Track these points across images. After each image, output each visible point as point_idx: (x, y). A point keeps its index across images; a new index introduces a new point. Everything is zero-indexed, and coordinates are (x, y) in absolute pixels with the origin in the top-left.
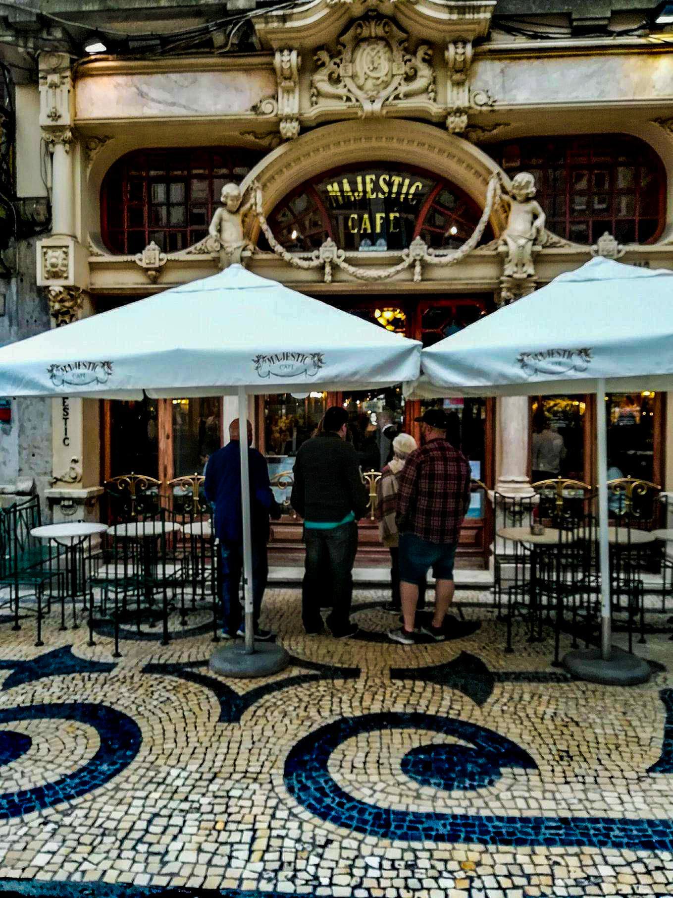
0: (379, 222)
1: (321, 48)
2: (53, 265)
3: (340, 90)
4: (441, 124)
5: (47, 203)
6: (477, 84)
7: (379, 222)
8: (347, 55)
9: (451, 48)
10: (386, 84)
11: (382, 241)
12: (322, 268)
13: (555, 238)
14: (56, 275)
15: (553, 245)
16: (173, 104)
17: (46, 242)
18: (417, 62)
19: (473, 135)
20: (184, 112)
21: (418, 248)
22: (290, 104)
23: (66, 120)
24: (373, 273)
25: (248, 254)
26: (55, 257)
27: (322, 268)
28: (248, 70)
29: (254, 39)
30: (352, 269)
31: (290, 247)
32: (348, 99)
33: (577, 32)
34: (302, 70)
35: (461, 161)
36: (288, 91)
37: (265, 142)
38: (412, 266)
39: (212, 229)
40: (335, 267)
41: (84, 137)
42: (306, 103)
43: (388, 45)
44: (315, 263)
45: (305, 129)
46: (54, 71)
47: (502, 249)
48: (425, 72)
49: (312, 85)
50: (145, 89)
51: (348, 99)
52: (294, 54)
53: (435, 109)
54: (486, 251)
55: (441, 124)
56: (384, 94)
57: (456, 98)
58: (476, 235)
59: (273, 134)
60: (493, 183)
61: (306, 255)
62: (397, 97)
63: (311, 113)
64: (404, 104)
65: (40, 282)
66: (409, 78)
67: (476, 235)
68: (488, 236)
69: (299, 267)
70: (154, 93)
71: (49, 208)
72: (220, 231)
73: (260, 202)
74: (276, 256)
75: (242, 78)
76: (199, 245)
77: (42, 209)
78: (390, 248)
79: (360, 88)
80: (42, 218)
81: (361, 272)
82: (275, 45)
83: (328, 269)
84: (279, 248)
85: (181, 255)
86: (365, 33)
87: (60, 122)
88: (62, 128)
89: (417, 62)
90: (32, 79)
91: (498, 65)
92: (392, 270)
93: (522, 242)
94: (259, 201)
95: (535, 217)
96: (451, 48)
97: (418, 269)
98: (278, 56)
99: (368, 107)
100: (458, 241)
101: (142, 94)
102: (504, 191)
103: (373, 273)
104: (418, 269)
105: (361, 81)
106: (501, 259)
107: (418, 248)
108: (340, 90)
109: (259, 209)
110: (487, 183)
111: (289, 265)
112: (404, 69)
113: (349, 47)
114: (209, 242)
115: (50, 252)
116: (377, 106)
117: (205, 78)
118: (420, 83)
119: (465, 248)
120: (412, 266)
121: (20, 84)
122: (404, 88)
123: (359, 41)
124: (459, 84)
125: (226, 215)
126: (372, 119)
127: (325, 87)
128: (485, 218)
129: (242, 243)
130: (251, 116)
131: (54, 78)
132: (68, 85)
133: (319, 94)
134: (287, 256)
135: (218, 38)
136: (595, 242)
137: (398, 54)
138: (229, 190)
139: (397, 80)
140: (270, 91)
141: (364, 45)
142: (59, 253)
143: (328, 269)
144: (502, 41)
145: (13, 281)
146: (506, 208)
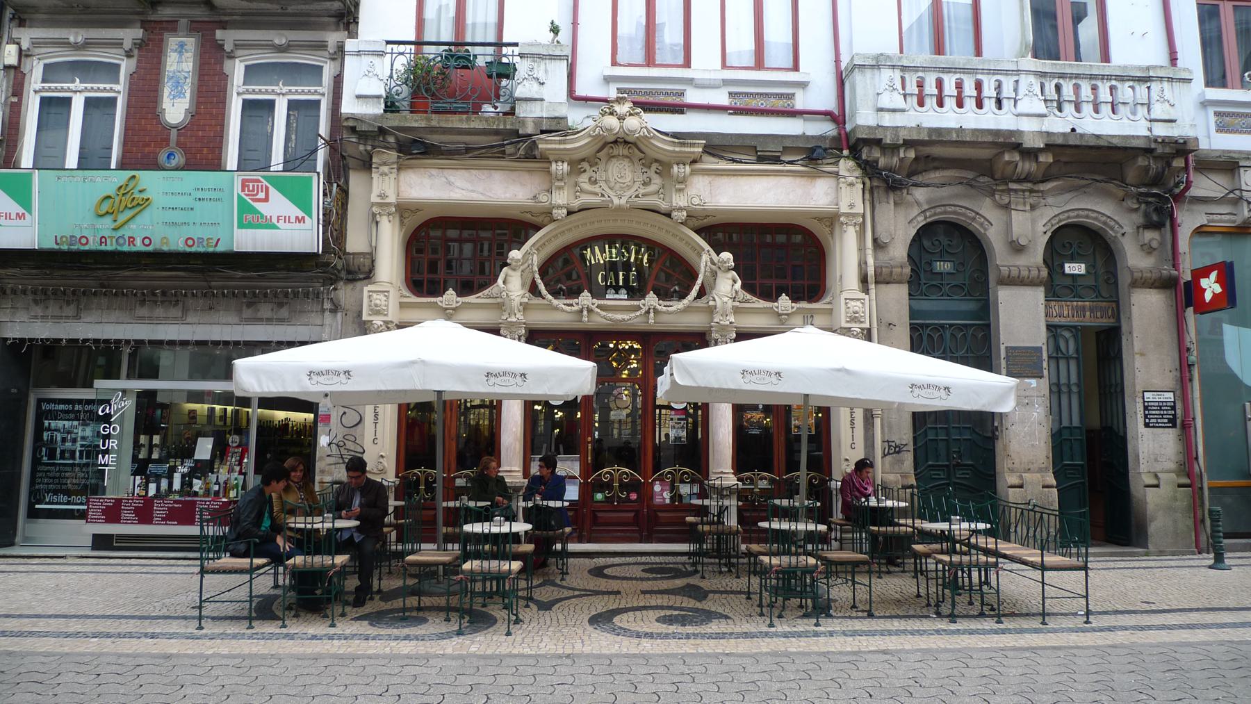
0: (621, 277)
1: (583, 160)
2: (376, 305)
3: (596, 189)
4: (668, 215)
5: (371, 257)
6: (692, 191)
7: (621, 277)
8: (602, 166)
9: (675, 167)
10: (629, 187)
11: (624, 291)
12: (581, 311)
13: (749, 296)
14: (378, 313)
15: (748, 301)
16: (473, 191)
17: (370, 287)
18: (651, 173)
19: (690, 223)
20: (482, 198)
21: (651, 299)
22: (562, 198)
23: (392, 199)
24: (619, 316)
25: (526, 300)
26: (379, 299)
27: (581, 311)
28: (530, 171)
29: (536, 153)
30: (603, 313)
31: (556, 294)
32: (603, 195)
33: (761, 160)
34: (570, 174)
35: (682, 239)
36: (560, 188)
37: (538, 220)
38: (648, 312)
39: (500, 281)
40: (590, 311)
41: (403, 210)
42: (572, 197)
43: (631, 161)
44: (576, 308)
45: (570, 213)
46: (385, 164)
47: (711, 303)
48: (657, 181)
49: (576, 184)
50: (452, 179)
51: (603, 195)
52: (566, 165)
53: (664, 206)
54: (701, 303)
55: (668, 215)
56: (628, 194)
57: (680, 201)
58: (694, 293)
59: (548, 214)
60: (705, 257)
61: (568, 301)
62: (637, 196)
63: (576, 204)
64: (643, 201)
65: (365, 318)
66: (645, 184)
67: (694, 293)
68: (702, 293)
69: (563, 311)
70: (458, 183)
71: (373, 261)
72: (504, 282)
73: (536, 261)
74: (545, 302)
75: (526, 177)
76: (486, 292)
77: (368, 262)
78: (631, 297)
79: (611, 189)
80: (367, 269)
81: (609, 315)
82: (551, 158)
83: (585, 313)
84: (550, 297)
85: (471, 299)
86: (615, 152)
87: (387, 201)
88: (388, 205)
89: (651, 173)
90: (366, 165)
91: (707, 179)
92: (633, 315)
93: (726, 299)
94: (535, 263)
95: (735, 282)
96: (675, 167)
97: (652, 315)
98: (554, 166)
99: (616, 201)
100: (682, 296)
101: (450, 183)
102: (713, 263)
103: (619, 316)
104: (652, 315)
105: (612, 185)
106: (711, 310)
107: (651, 299)
108: (596, 189)
109: (536, 269)
110: (701, 256)
111: (556, 308)
112: (642, 178)
113: (604, 160)
114: (491, 290)
115: (375, 295)
116: (623, 201)
117: (497, 175)
118: (652, 188)
119: (685, 301)
120: (648, 312)
121: (355, 169)
122: (641, 191)
123: (611, 157)
124: (681, 190)
125: (511, 272)
126: (619, 209)
127: (587, 186)
128: (699, 281)
129: (521, 292)
130: (531, 203)
131: (385, 169)
132: (394, 175)
133: (582, 191)
134: (555, 302)
135: (509, 149)
136: (776, 300)
137: (638, 167)
138: (515, 254)
139: (637, 184)
140: (546, 187)
141: (614, 160)
142: (381, 296)
143: (585, 313)
144: (710, 163)
145: (339, 315)
146: (714, 274)
